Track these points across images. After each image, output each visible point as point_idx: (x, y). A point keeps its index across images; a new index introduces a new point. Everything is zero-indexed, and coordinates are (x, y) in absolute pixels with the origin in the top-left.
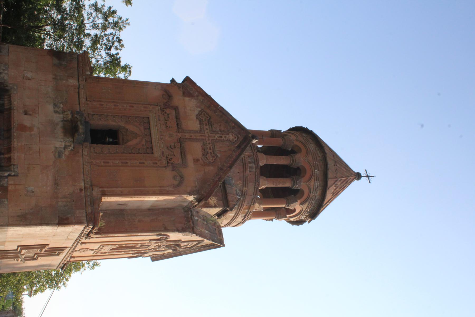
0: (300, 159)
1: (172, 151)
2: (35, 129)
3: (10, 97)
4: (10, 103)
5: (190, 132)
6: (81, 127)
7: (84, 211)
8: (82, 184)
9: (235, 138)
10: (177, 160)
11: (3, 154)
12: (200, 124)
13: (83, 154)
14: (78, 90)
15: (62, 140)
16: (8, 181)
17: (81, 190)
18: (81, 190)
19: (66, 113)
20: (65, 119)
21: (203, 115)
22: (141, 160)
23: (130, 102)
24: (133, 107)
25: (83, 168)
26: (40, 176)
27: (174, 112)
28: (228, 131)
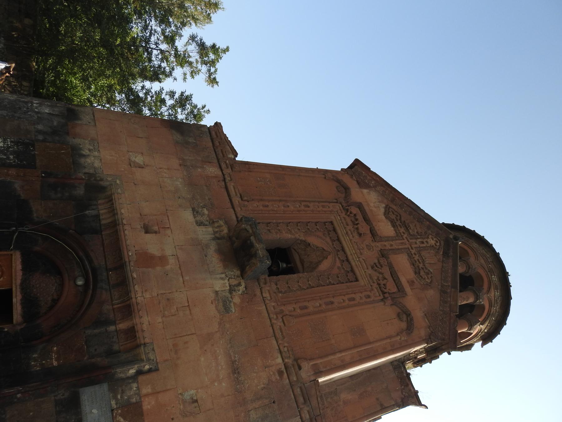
1: (380, 273)
2: (172, 260)
3: (110, 200)
4: (113, 211)
5: (388, 239)
6: (257, 245)
8: (279, 360)
9: (437, 242)
11: (114, 323)
13: (263, 298)
14: (223, 184)
15: (223, 276)
16: (138, 388)
18: (280, 373)
19: (216, 225)
20: (217, 235)
21: (391, 213)
24: (309, 207)
25: (272, 326)
26: (202, 359)
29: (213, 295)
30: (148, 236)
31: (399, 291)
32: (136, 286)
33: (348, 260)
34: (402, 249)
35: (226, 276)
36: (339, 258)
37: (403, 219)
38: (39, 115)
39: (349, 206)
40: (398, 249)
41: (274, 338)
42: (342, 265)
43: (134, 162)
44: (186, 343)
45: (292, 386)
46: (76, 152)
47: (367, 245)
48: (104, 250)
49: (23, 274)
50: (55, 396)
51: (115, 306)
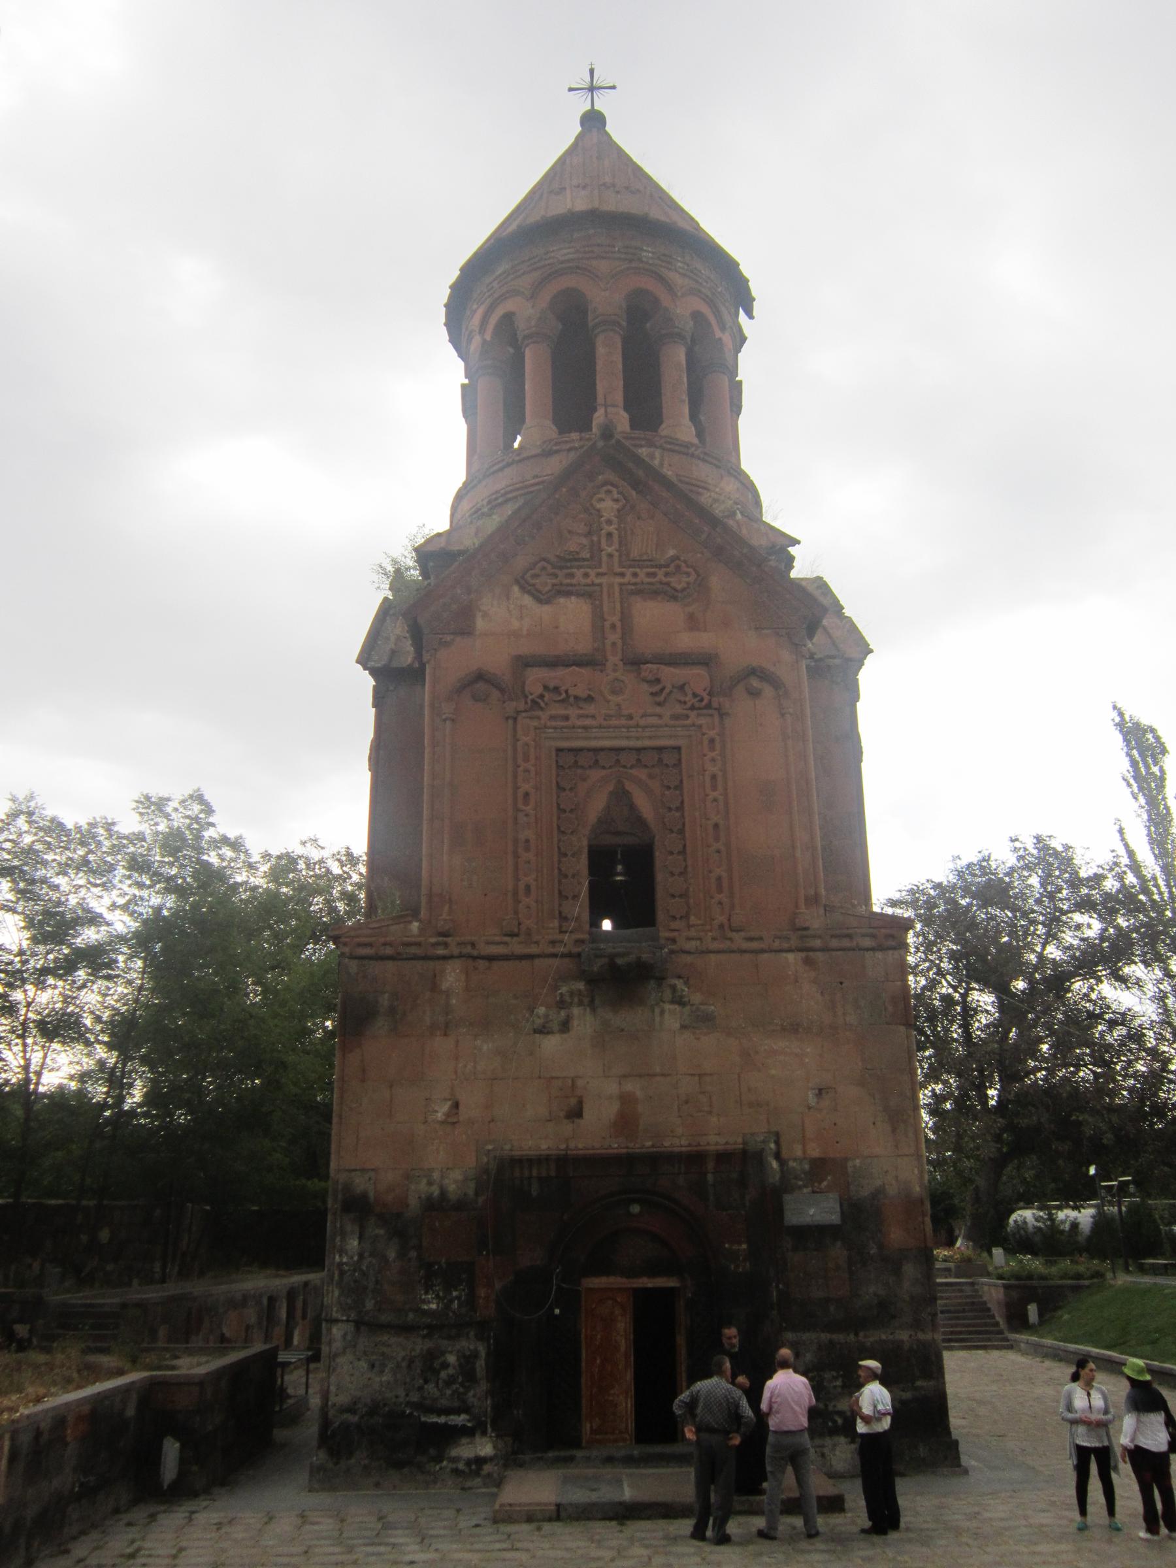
2: (629, 1086)
7: (868, 954)
8: (791, 957)
9: (609, 492)
10: (697, 678)
12: (568, 594)
14: (481, 961)
15: (657, 1010)
16: (795, 1160)
17: (808, 962)
19: (568, 999)
20: (586, 1001)
24: (527, 795)
26: (773, 1072)
27: (535, 670)
31: (707, 664)
32: (666, 1144)
33: (639, 750)
34: (621, 603)
35: (657, 1004)
36: (632, 767)
38: (366, 1254)
39: (526, 697)
40: (622, 613)
42: (646, 766)
43: (448, 1115)
44: (749, 1090)
45: (825, 949)
46: (436, 1206)
47: (614, 692)
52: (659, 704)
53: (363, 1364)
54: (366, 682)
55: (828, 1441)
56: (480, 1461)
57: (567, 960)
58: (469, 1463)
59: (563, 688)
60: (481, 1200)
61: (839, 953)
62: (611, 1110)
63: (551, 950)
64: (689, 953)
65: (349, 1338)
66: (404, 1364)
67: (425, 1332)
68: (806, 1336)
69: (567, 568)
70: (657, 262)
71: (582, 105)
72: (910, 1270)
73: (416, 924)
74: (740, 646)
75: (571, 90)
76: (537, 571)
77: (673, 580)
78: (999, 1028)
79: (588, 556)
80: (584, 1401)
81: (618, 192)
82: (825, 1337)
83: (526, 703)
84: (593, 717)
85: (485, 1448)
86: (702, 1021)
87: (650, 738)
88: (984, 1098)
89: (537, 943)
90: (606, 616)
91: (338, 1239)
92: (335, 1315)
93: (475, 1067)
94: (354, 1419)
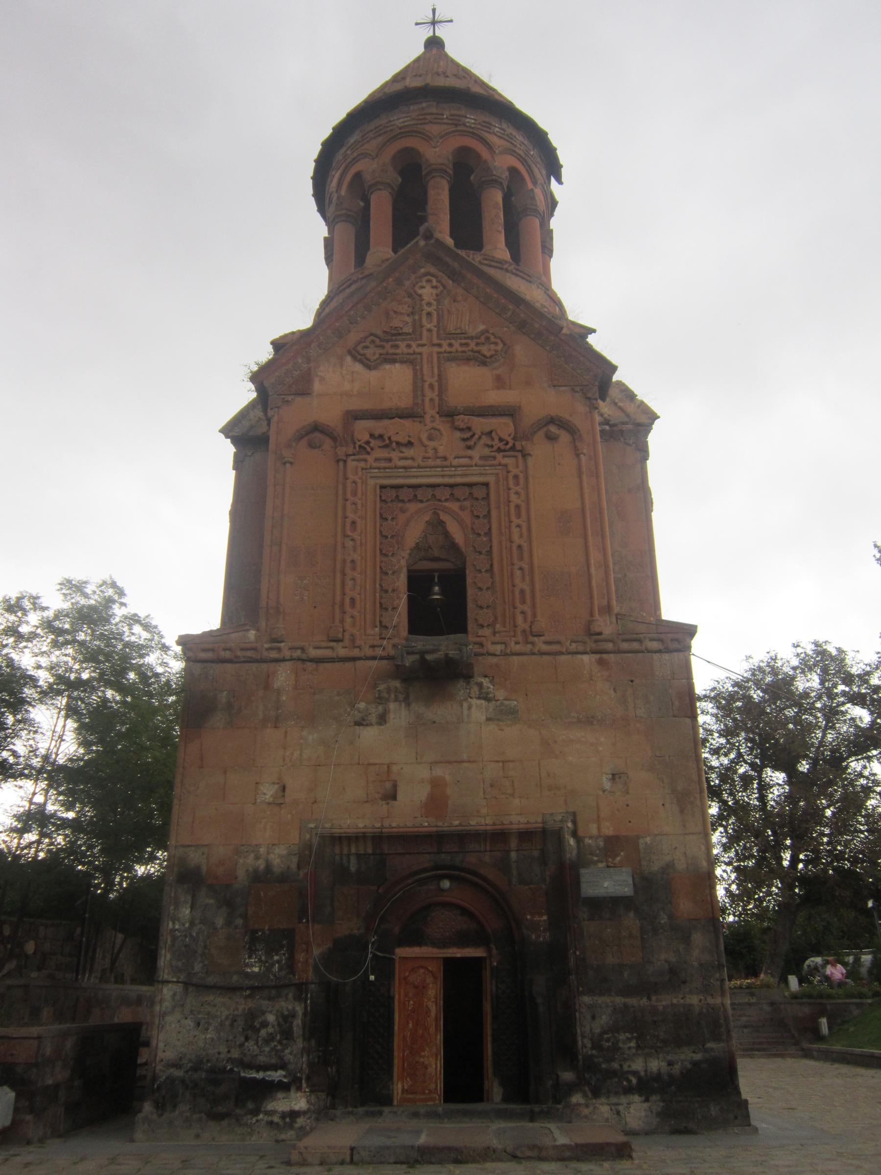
0: (437, 153)
1: (480, 438)
2: (439, 772)
3: (338, 839)
7: (656, 656)
8: (586, 658)
9: (429, 281)
10: (504, 427)
12: (394, 361)
14: (309, 664)
15: (465, 705)
16: (591, 837)
17: (601, 662)
20: (401, 697)
21: (366, 351)
22: (509, 514)
23: (339, 529)
26: (570, 758)
27: (362, 421)
28: (410, 295)
29: (492, 727)
30: (400, 796)
32: (472, 823)
33: (452, 486)
34: (439, 367)
35: (466, 700)
36: (446, 500)
37: (379, 332)
38: (197, 922)
39: (355, 443)
40: (439, 375)
41: (558, 657)
42: (458, 500)
44: (549, 775)
45: (619, 651)
47: (430, 438)
48: (410, 854)
49: (426, 945)
50: (584, 920)
51: (488, 848)
52: (469, 448)
53: (190, 1023)
54: (228, 450)
55: (624, 1100)
56: (294, 1115)
57: (384, 662)
58: (283, 1116)
59: (386, 437)
60: (301, 873)
61: (630, 655)
62: (422, 793)
63: (370, 652)
64: (494, 655)
65: (178, 997)
66: (227, 1023)
67: (248, 992)
68: (600, 1000)
69: (392, 341)
70: (479, 126)
71: (426, 33)
72: (699, 938)
73: (254, 632)
74: (539, 400)
75: (417, 24)
76: (367, 344)
77: (485, 350)
78: (790, 798)
79: (411, 331)
80: (396, 1061)
81: (447, 77)
82: (619, 1000)
83: (355, 448)
84: (413, 459)
85: (299, 1102)
86: (505, 715)
87: (462, 475)
88: (780, 859)
89: (359, 647)
90: (426, 378)
91: (172, 907)
92: (166, 977)
93: (301, 755)
94: (179, 1073)
